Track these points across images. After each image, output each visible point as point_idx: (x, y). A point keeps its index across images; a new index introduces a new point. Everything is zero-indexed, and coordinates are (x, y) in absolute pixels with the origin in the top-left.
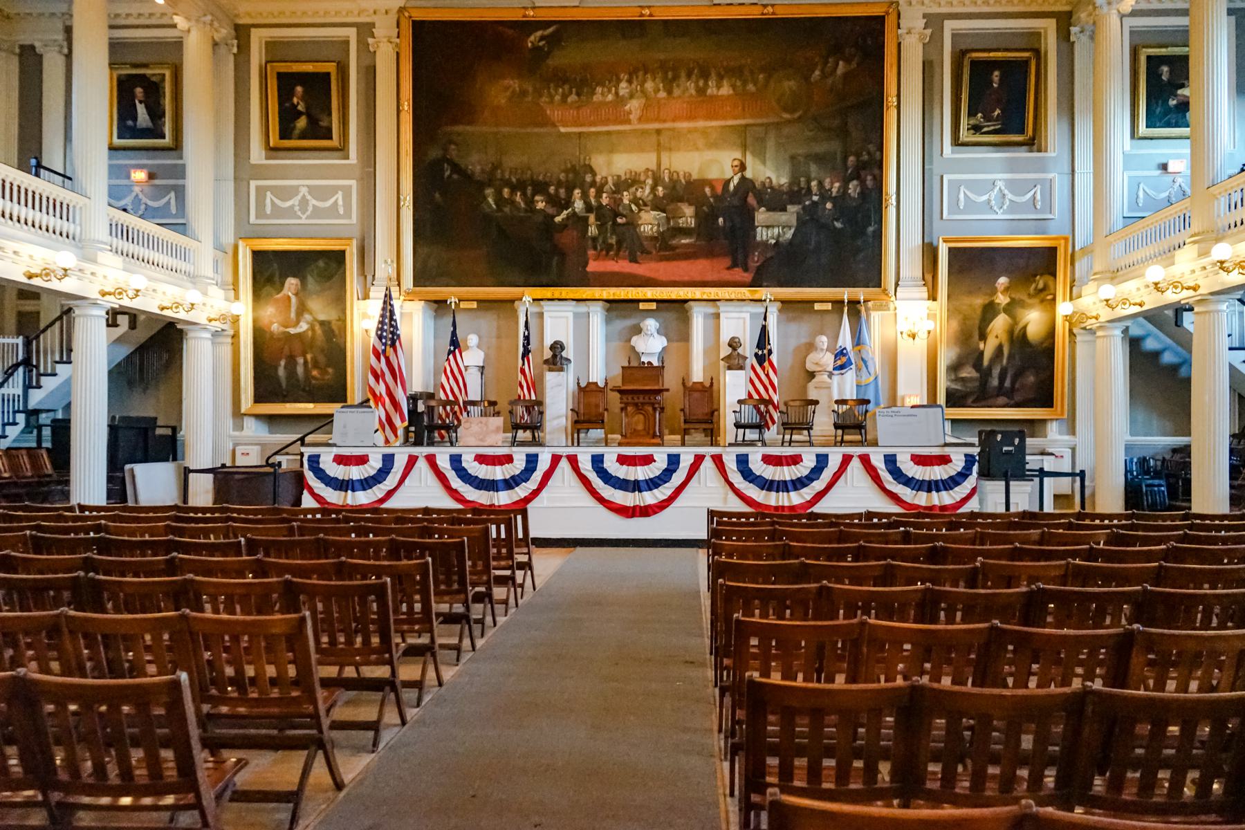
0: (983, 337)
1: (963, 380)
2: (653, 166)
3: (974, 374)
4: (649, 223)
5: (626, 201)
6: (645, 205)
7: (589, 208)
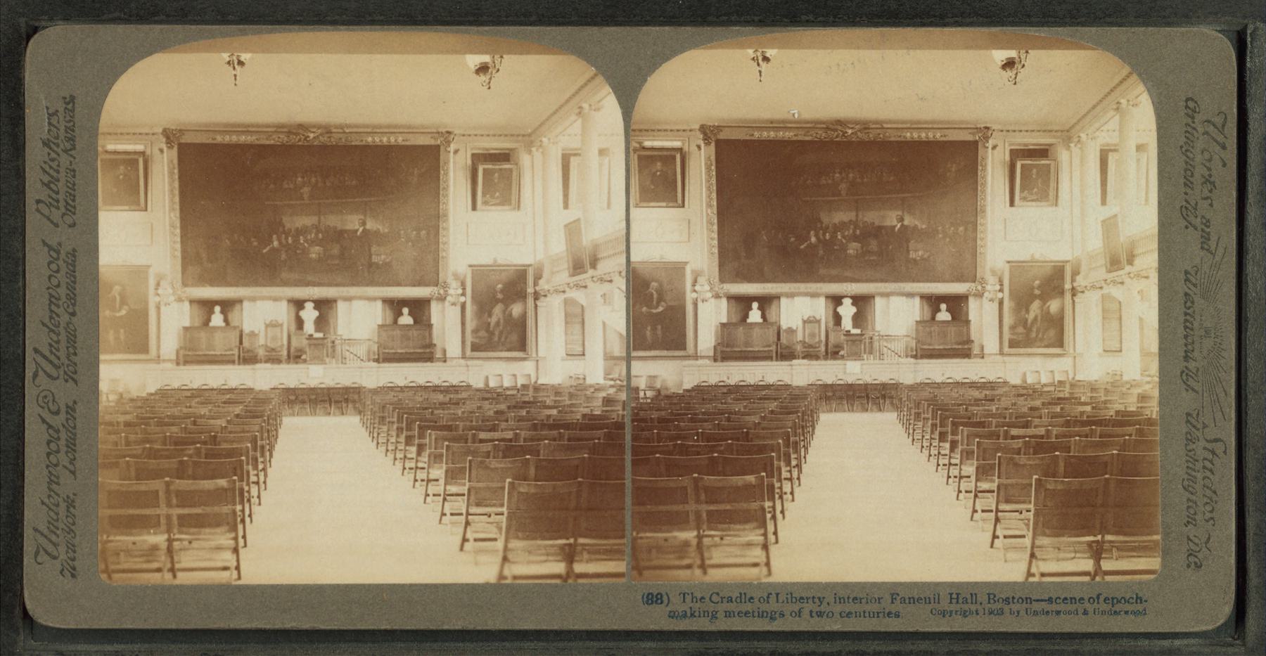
0: (490, 315)
1: (480, 338)
2: (317, 223)
3: (486, 335)
4: (315, 252)
5: (302, 241)
6: (313, 242)
7: (280, 243)
